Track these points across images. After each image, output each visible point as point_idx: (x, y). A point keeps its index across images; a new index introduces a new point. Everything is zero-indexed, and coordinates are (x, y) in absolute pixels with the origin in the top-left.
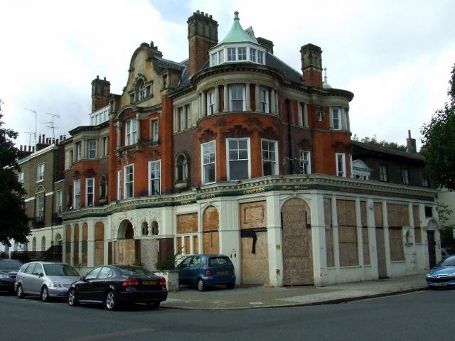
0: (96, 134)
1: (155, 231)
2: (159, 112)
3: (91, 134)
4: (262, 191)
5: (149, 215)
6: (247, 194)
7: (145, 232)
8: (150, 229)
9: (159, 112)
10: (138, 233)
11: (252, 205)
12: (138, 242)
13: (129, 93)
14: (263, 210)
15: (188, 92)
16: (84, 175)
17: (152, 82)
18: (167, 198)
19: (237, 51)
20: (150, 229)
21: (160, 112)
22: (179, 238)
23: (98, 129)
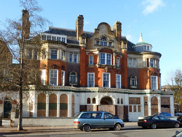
0: (65, 49)
1: (122, 103)
2: (120, 56)
3: (64, 48)
4: (169, 95)
5: (121, 96)
6: (164, 95)
7: (118, 103)
8: (120, 102)
9: (120, 56)
10: (115, 102)
11: (165, 98)
12: (116, 106)
13: (96, 39)
14: (168, 100)
15: (137, 54)
16: (61, 68)
17: (113, 41)
18: (128, 90)
19: (147, 47)
20: (120, 102)
21: (121, 56)
22: (131, 106)
23: (68, 47)
